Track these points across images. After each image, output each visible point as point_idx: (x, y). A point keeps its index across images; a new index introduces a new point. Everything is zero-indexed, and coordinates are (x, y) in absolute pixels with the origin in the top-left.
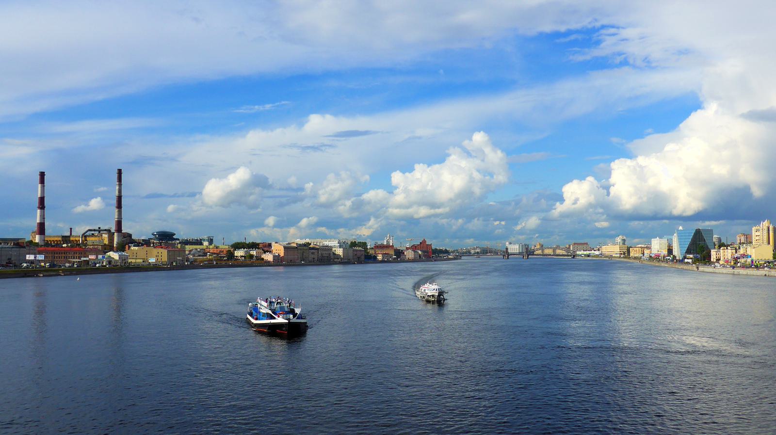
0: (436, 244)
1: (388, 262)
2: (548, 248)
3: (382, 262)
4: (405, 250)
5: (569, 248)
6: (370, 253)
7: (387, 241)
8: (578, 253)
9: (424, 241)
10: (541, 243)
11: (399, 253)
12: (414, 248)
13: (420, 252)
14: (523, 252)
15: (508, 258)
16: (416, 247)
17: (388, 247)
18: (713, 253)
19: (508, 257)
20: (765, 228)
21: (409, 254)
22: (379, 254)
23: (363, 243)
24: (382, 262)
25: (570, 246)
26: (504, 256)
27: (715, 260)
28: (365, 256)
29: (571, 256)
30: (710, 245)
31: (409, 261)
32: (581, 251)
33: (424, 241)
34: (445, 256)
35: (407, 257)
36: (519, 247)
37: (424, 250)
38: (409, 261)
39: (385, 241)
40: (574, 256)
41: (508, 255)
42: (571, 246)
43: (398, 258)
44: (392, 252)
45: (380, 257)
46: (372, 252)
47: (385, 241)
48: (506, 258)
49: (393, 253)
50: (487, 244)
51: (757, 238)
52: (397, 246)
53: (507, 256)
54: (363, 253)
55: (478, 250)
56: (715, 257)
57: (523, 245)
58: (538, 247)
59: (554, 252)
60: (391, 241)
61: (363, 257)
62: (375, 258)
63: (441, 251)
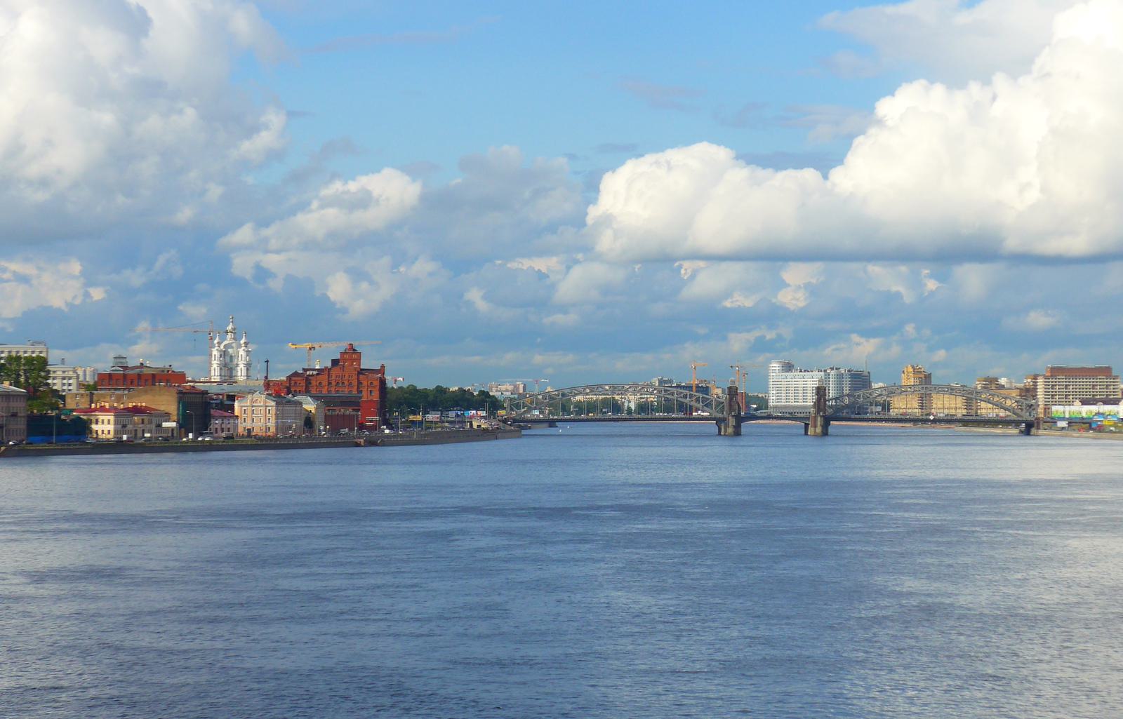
2: (952, 391)
3: (114, 447)
7: (224, 354)
8: (1057, 410)
9: (352, 354)
10: (926, 368)
11: (203, 413)
12: (282, 392)
13: (310, 405)
14: (767, 408)
15: (737, 433)
21: (255, 413)
22: (103, 409)
23: (30, 361)
24: (114, 447)
25: (1035, 377)
26: (719, 421)
29: (1016, 423)
32: (1071, 403)
33: (352, 354)
34: (478, 419)
39: (215, 352)
40: (1030, 426)
41: (740, 420)
42: (1041, 381)
44: (166, 402)
45: (105, 427)
46: (75, 403)
47: (215, 352)
48: (730, 430)
52: (207, 373)
53: (732, 422)
54: (20, 407)
57: (840, 376)
58: (908, 380)
59: (969, 403)
60: (242, 352)
61: (21, 425)
63: (464, 400)
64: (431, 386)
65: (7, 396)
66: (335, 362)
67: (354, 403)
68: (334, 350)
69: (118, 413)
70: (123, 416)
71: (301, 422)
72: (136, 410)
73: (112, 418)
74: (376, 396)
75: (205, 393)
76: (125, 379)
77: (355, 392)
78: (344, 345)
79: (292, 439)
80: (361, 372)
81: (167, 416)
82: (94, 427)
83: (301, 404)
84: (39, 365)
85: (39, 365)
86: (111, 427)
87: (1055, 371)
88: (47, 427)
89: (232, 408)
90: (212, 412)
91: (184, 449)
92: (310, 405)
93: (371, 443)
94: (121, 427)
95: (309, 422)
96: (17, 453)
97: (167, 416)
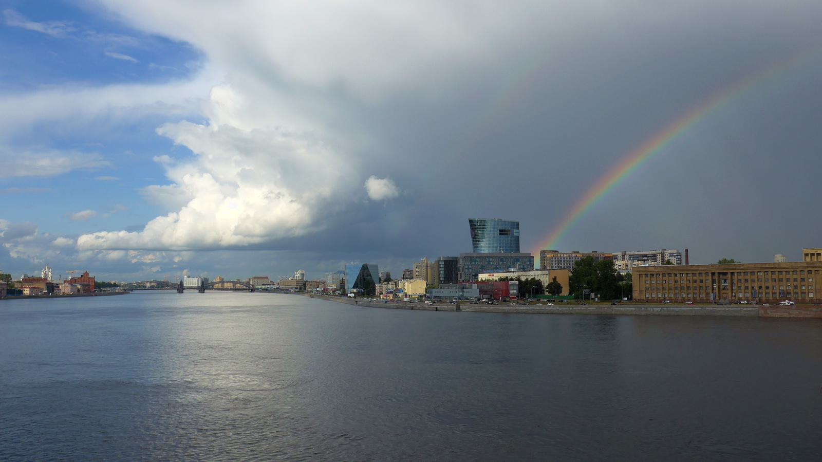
0: (100, 278)
1: (37, 297)
4: (61, 284)
5: (249, 282)
6: (16, 286)
9: (86, 274)
12: (73, 282)
13: (79, 287)
16: (75, 281)
17: (39, 280)
18: (377, 286)
19: (183, 291)
20: (424, 264)
21: (65, 288)
22: (26, 288)
23: (6, 275)
27: (378, 294)
28: (8, 290)
30: (375, 279)
31: (65, 296)
33: (86, 274)
34: (117, 290)
35: (63, 291)
36: (198, 281)
37: (85, 283)
38: (65, 296)
43: (49, 293)
44: (42, 286)
45: (27, 292)
46: (17, 286)
49: (44, 287)
50: (162, 278)
51: (417, 274)
55: (154, 284)
56: (378, 291)
62: (21, 292)
64: (106, 282)
65: (2, 284)
66: (82, 276)
67: (88, 286)
68: (82, 272)
69: (30, 289)
70: (32, 289)
71: (77, 290)
72: (34, 288)
73: (29, 290)
74: (93, 284)
75: (53, 283)
76: (28, 280)
77: (88, 283)
78: (85, 272)
79: (77, 294)
80: (89, 278)
81: (43, 289)
82: (24, 292)
83: (77, 286)
84: (9, 276)
85: (9, 276)
86: (29, 292)
87: (255, 278)
88: (13, 292)
89: (59, 287)
90: (55, 288)
91: (48, 297)
92: (79, 287)
93: (96, 295)
94: (31, 292)
95: (79, 290)
96: (6, 298)
97: (43, 289)
